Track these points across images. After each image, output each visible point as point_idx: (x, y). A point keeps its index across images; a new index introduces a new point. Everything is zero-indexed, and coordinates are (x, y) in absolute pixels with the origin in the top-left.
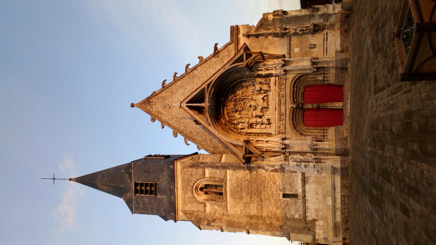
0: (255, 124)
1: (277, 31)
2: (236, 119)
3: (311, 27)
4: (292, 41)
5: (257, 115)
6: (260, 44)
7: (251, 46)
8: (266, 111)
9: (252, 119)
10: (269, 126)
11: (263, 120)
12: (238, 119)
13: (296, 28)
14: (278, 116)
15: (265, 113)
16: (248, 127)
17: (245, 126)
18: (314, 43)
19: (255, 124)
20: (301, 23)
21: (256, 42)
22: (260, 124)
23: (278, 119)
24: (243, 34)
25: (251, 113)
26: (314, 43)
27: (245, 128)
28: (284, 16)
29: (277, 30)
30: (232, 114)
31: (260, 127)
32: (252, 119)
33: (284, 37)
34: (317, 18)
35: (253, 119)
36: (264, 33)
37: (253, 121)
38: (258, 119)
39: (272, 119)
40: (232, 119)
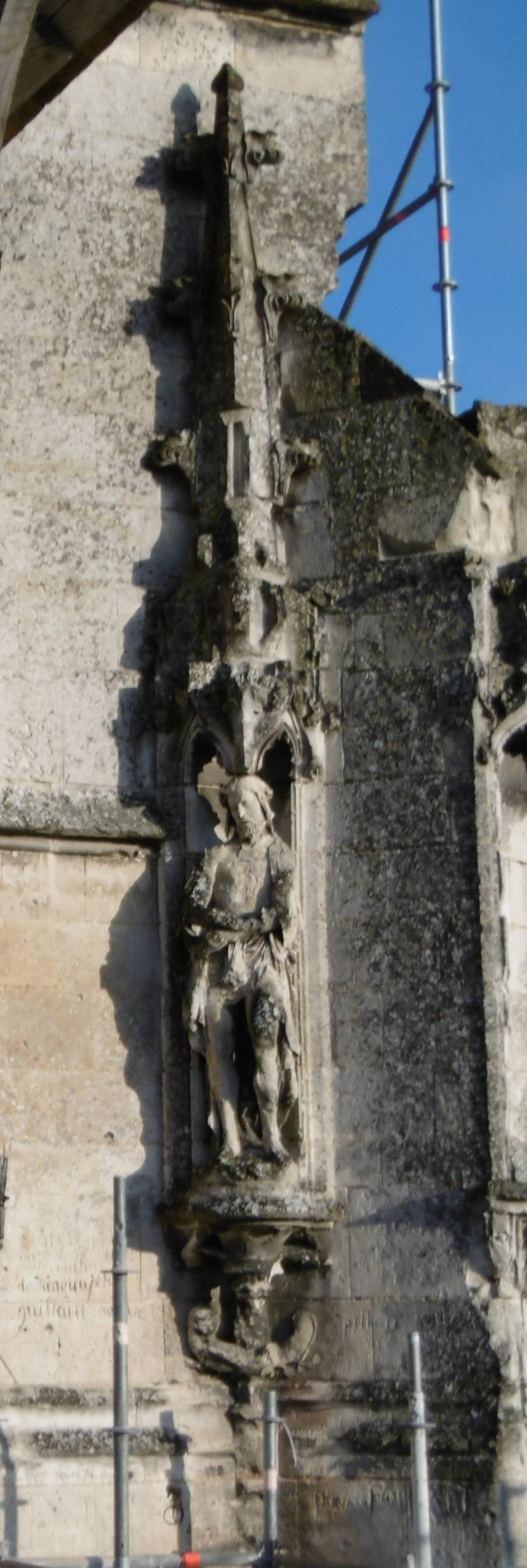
1: (255, 630)
3: (294, 1173)
4: (73, 869)
6: (60, 346)
7: (45, 188)
13: (289, 936)
18: (25, 1240)
20: (364, 1021)
21: (101, 280)
24: (239, 85)
26: (25, 1240)
28: (500, 740)
29: (271, 622)
33: (145, 757)
34: (428, 1280)
36: (228, 419)
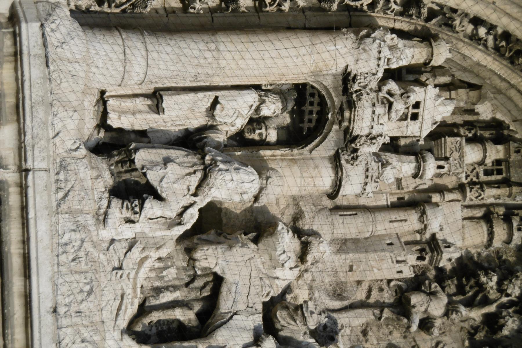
0: (263, 144)
2: (461, 188)
5: (252, 246)
8: (158, 291)
9: (296, 200)
10: (122, 113)
11: (195, 180)
12: (440, 190)
14: (26, 242)
15: (171, 274)
16: (346, 91)
17: (380, 110)
19: (263, 144)
22: (221, 138)
23: (24, 208)
25: (315, 262)
27: (383, 81)
30: (508, 241)
31: (216, 102)
32: (310, 189)
35: (295, 191)
37: (296, 170)
38: (249, 197)
39: (90, 206)
40: (503, 191)
